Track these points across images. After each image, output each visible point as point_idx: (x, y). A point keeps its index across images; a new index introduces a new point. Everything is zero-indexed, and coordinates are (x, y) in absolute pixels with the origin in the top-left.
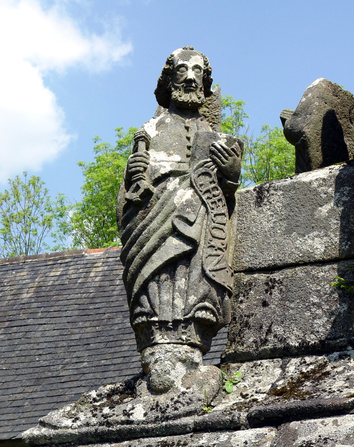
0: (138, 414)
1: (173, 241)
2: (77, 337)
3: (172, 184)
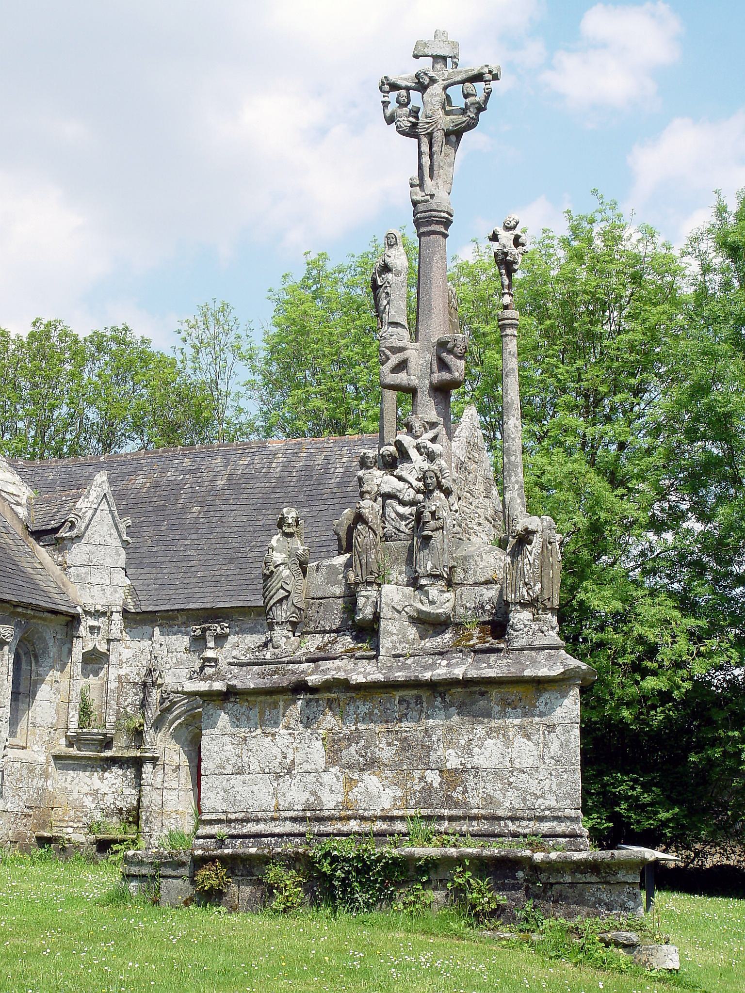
0: (268, 657)
1: (282, 591)
2: (261, 523)
3: (282, 567)
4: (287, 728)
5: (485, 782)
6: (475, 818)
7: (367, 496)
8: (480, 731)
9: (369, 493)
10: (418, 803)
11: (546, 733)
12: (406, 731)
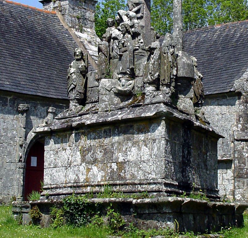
1: (72, 85)
2: (202, 61)
4: (70, 146)
5: (132, 168)
6: (127, 184)
7: (104, 39)
8: (130, 144)
9: (105, 38)
10: (109, 178)
11: (153, 143)
12: (106, 145)
